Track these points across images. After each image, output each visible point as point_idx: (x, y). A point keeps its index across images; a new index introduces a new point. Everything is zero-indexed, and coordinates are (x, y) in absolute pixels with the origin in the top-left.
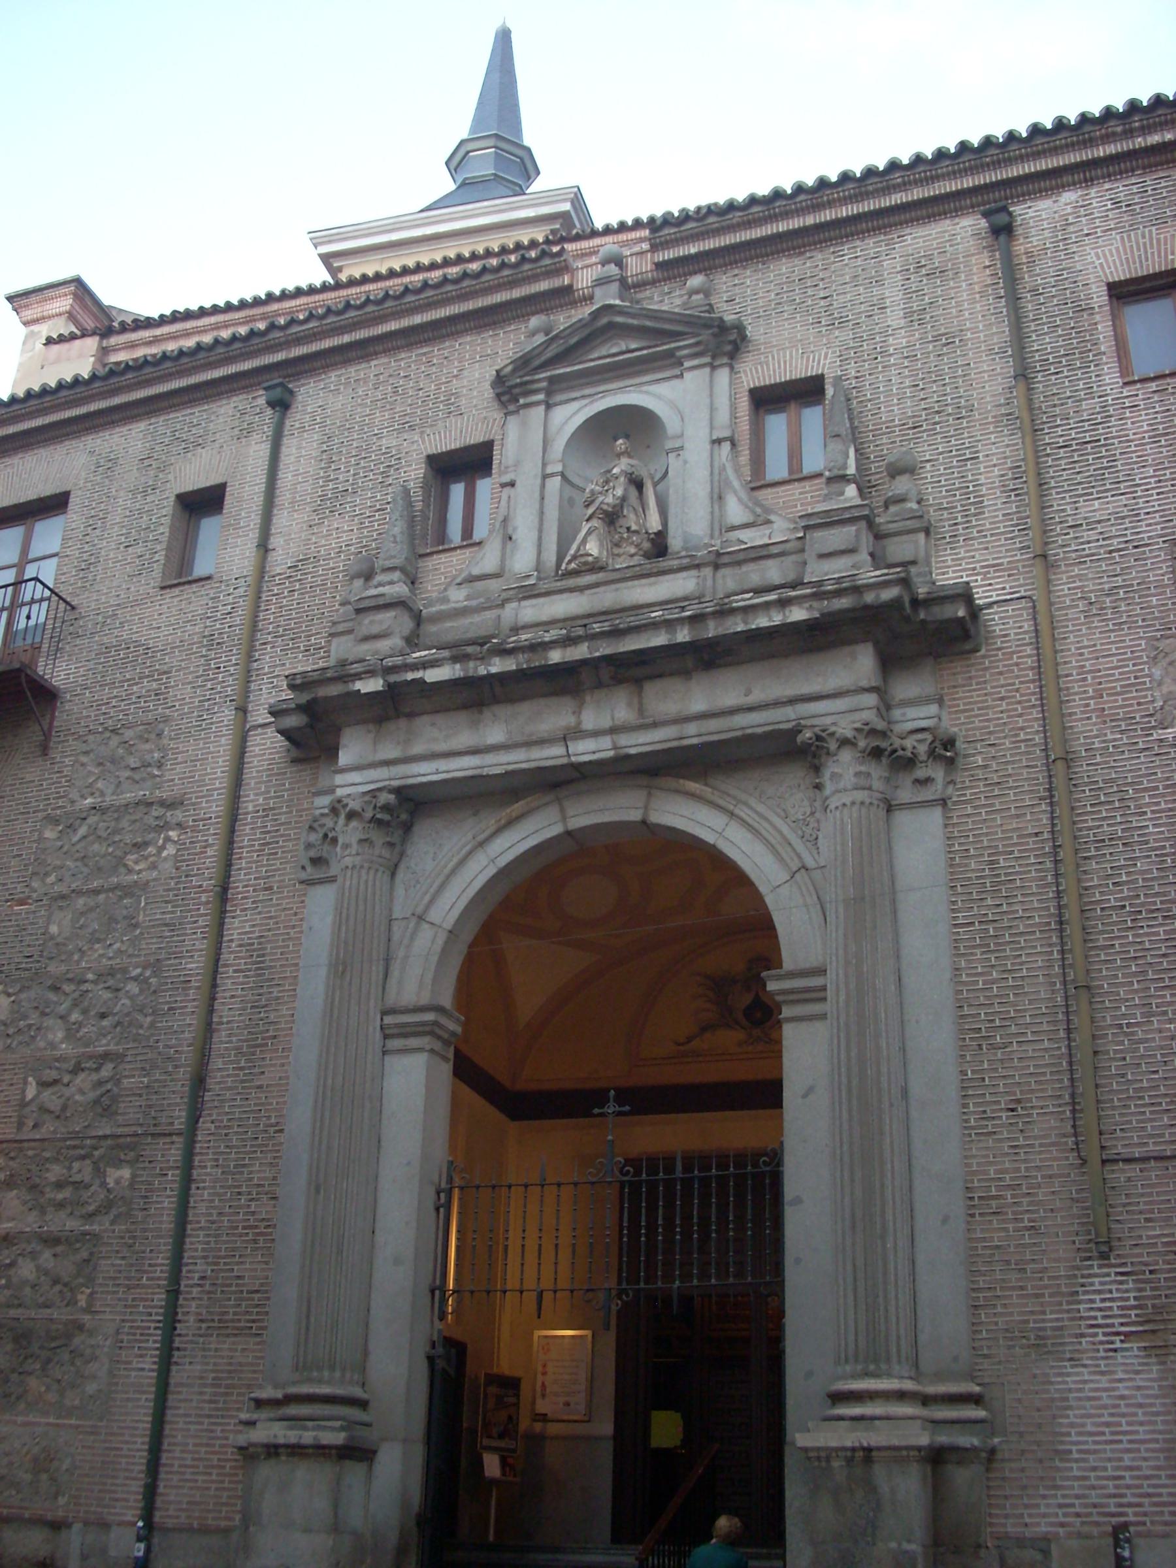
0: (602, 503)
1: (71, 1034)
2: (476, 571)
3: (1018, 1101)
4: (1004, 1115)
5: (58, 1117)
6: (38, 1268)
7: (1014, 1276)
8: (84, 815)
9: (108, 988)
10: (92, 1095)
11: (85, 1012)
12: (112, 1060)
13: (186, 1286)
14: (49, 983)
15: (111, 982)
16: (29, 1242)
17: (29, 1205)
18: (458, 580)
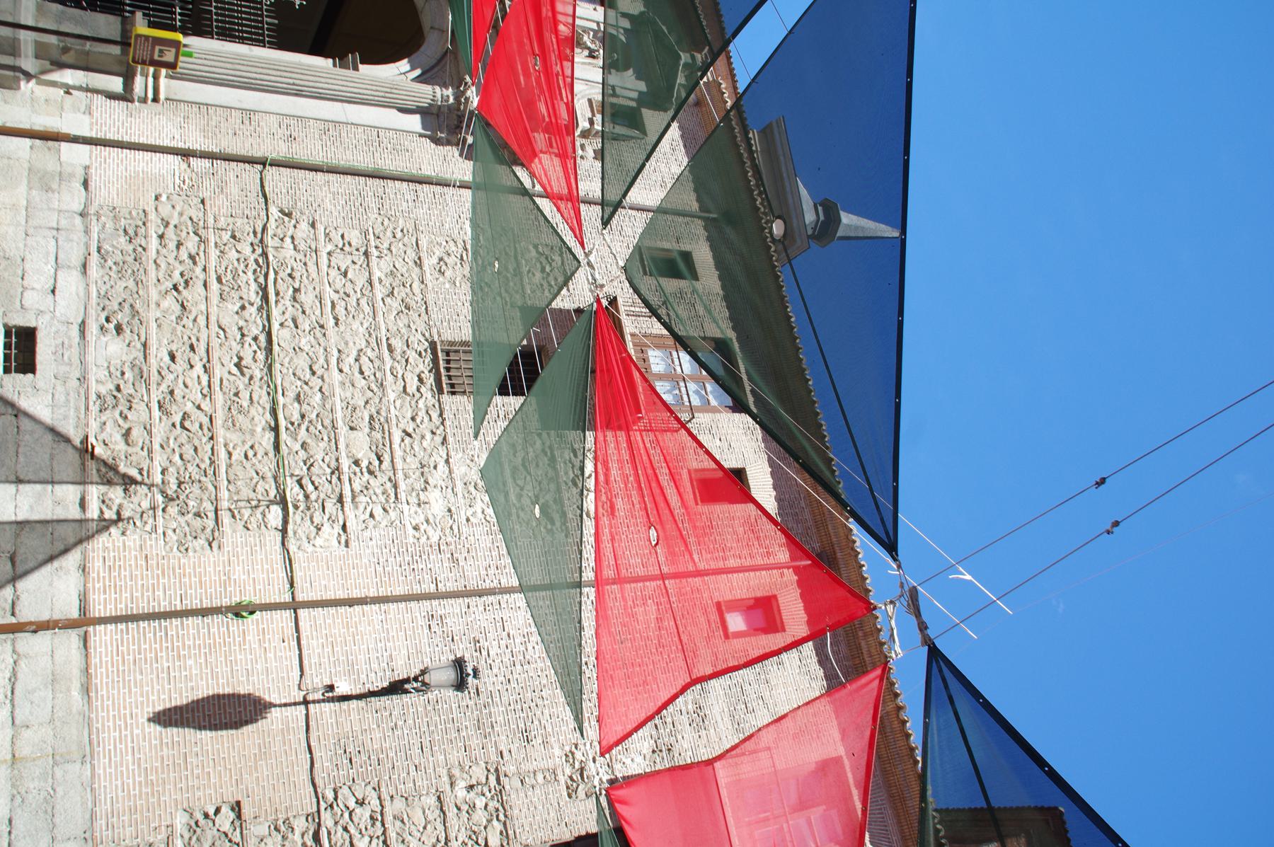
4: (289, 133)
7: (214, 124)
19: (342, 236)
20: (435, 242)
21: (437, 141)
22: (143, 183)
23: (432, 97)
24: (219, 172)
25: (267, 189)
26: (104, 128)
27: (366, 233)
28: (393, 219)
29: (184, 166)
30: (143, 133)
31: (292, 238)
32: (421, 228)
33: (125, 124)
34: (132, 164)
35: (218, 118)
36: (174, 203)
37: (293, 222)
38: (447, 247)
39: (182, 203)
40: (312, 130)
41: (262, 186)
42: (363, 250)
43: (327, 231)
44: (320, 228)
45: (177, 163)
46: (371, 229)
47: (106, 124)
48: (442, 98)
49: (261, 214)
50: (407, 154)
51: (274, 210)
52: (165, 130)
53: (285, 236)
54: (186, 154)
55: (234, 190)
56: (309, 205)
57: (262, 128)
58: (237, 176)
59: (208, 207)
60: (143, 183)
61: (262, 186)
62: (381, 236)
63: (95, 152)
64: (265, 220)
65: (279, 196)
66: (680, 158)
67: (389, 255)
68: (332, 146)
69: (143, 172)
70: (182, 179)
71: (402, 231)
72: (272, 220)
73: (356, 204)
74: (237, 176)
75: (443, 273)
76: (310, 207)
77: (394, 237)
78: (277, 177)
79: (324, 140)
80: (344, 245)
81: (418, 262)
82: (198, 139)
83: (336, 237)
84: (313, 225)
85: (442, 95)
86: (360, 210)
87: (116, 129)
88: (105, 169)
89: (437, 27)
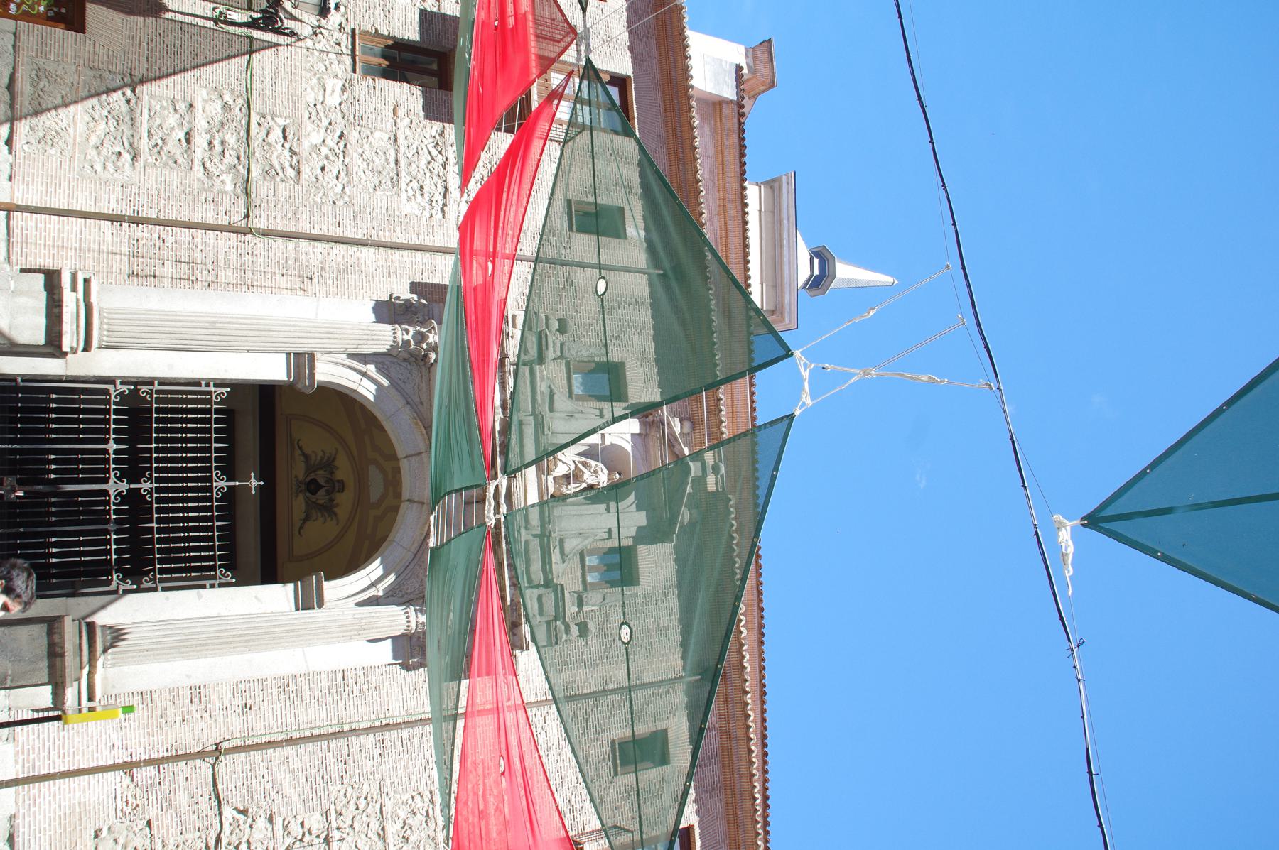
0: (583, 472)
1: (316, 149)
2: (556, 397)
3: (250, 709)
4: (244, 702)
5: (264, 140)
6: (173, 129)
7: (159, 713)
8: (443, 153)
9: (339, 172)
10: (276, 163)
11: (327, 157)
12: (296, 176)
13: (160, 230)
15: (343, 174)
16: (189, 122)
18: (553, 387)
19: (302, 824)
20: (401, 802)
21: (407, 667)
22: (80, 819)
23: (406, 628)
24: (167, 779)
25: (220, 787)
26: (32, 757)
27: (327, 813)
28: (357, 786)
29: (127, 780)
30: (78, 749)
31: (248, 842)
32: (386, 791)
33: (57, 743)
34: (67, 796)
35: (164, 704)
36: (116, 836)
37: (250, 820)
38: (413, 805)
39: (125, 832)
40: (270, 691)
41: (215, 785)
42: (324, 835)
43: (286, 823)
44: (278, 821)
45: (118, 779)
46: (332, 807)
47: (33, 749)
48: (417, 626)
49: (214, 822)
50: (374, 693)
51: (228, 813)
52: (104, 737)
53: (240, 843)
54: (127, 767)
55: (183, 799)
56: (267, 794)
57: (214, 704)
58: (187, 778)
59: (155, 831)
60: (80, 819)
61: (215, 785)
62: (343, 812)
63: (22, 794)
64: (219, 829)
65: (234, 793)
66: (671, 604)
67: (352, 834)
68: (292, 706)
69: (80, 804)
70: (124, 799)
71: (366, 798)
72: (226, 825)
73: (318, 778)
74: (187, 778)
75: (407, 839)
76: (267, 798)
77: (357, 809)
78: (231, 768)
79: (283, 700)
80: (304, 835)
81: (382, 833)
82: (142, 740)
83: (296, 830)
84: (270, 819)
85: (417, 622)
86: (322, 785)
87: (46, 753)
88: (34, 813)
89: (416, 499)
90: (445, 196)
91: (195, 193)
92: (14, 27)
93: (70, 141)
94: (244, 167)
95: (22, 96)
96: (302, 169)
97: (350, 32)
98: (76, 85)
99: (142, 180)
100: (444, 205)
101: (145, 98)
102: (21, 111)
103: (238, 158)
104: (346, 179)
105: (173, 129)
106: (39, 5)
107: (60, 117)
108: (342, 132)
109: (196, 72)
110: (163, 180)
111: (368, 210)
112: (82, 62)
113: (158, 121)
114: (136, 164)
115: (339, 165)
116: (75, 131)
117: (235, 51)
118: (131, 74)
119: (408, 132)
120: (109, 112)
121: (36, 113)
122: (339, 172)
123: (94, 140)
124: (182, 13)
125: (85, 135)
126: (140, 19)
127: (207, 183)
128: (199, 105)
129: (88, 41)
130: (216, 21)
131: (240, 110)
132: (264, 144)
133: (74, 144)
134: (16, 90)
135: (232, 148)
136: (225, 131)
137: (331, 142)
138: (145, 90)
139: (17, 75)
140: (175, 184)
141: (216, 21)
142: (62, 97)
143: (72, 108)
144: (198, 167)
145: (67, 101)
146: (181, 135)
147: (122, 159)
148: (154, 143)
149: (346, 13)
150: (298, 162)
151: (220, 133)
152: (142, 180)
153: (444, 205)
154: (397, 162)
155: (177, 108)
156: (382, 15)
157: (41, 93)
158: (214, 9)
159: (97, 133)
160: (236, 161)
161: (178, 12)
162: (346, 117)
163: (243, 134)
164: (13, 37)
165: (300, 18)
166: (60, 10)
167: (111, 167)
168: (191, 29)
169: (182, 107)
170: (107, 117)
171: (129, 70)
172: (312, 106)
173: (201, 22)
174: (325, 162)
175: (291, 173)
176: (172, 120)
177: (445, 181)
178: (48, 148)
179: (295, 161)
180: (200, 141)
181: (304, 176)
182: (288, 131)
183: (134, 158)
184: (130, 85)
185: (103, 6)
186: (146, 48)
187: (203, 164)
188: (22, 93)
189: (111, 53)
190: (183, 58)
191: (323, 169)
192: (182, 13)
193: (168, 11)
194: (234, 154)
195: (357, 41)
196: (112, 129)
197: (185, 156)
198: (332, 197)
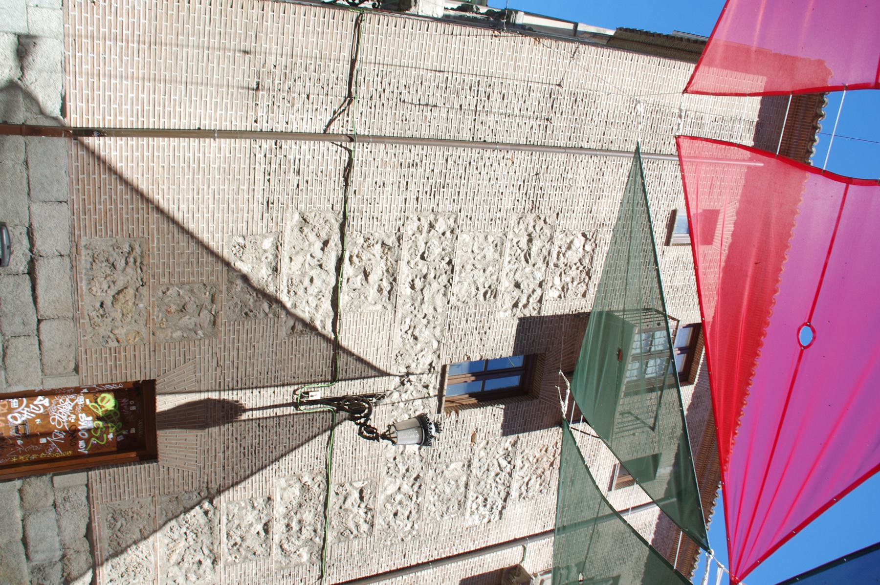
1: (390, 498)
5: (341, 508)
6: (251, 525)
9: (410, 512)
11: (400, 503)
12: (369, 529)
14: (421, 475)
16: (267, 515)
17: (290, 506)
90: (505, 500)
91: (274, 573)
92: (86, 479)
93: (152, 567)
94: (320, 538)
95: (101, 542)
96: (376, 522)
97: (440, 370)
98: (152, 515)
99: (223, 578)
100: (503, 508)
101: (223, 506)
102: (101, 555)
103: (315, 531)
104: (416, 516)
105: (251, 525)
106: (108, 434)
107: (140, 549)
108: (418, 475)
109: (275, 466)
110: (243, 572)
111: (433, 536)
112: (157, 492)
113: (237, 522)
114: (217, 567)
115: (412, 505)
116: (156, 556)
117: (315, 430)
118: (208, 488)
119: (483, 454)
120: (188, 528)
121: (116, 554)
122: (410, 512)
123: (175, 558)
124: (259, 409)
125: (165, 557)
126: (215, 430)
127: (284, 562)
128: (277, 497)
129: (161, 470)
130: (296, 405)
131: (319, 486)
132: (341, 511)
133: (156, 568)
134: (95, 538)
135: (310, 524)
136: (302, 511)
137: (406, 488)
138: (222, 501)
139: (93, 525)
140: (254, 572)
141: (296, 405)
142: (141, 531)
143: (151, 539)
144: (276, 550)
145: (146, 535)
146: (259, 527)
147: (203, 567)
148: (232, 542)
149: (438, 349)
150: (373, 517)
151: (299, 515)
152: (223, 578)
153: (503, 508)
154: (467, 486)
155: (256, 505)
156: (478, 339)
157: (119, 534)
158: (294, 392)
159: (177, 552)
160: (313, 534)
161: (256, 409)
162: (424, 460)
163: (321, 508)
164: (85, 489)
165: (388, 371)
166: (129, 431)
167: (193, 577)
168: (270, 423)
169: (260, 502)
170: (185, 533)
171: (205, 485)
172: (392, 460)
173: (279, 411)
174: (399, 508)
175: (364, 527)
176: (251, 517)
177: (509, 487)
178: (131, 580)
179: (369, 516)
180: (278, 528)
181: (377, 527)
182: (365, 491)
183: (214, 562)
184: (206, 498)
185: (175, 428)
186: (222, 456)
187: (281, 547)
188: (100, 539)
189: (186, 473)
190: (261, 455)
191: (395, 514)
192: (259, 409)
193: (245, 411)
194: (311, 528)
195: (446, 380)
196: (192, 543)
197: (264, 545)
198: (401, 535)
